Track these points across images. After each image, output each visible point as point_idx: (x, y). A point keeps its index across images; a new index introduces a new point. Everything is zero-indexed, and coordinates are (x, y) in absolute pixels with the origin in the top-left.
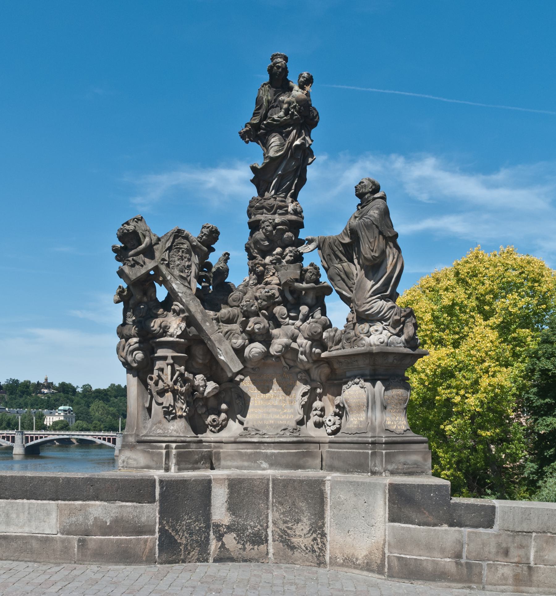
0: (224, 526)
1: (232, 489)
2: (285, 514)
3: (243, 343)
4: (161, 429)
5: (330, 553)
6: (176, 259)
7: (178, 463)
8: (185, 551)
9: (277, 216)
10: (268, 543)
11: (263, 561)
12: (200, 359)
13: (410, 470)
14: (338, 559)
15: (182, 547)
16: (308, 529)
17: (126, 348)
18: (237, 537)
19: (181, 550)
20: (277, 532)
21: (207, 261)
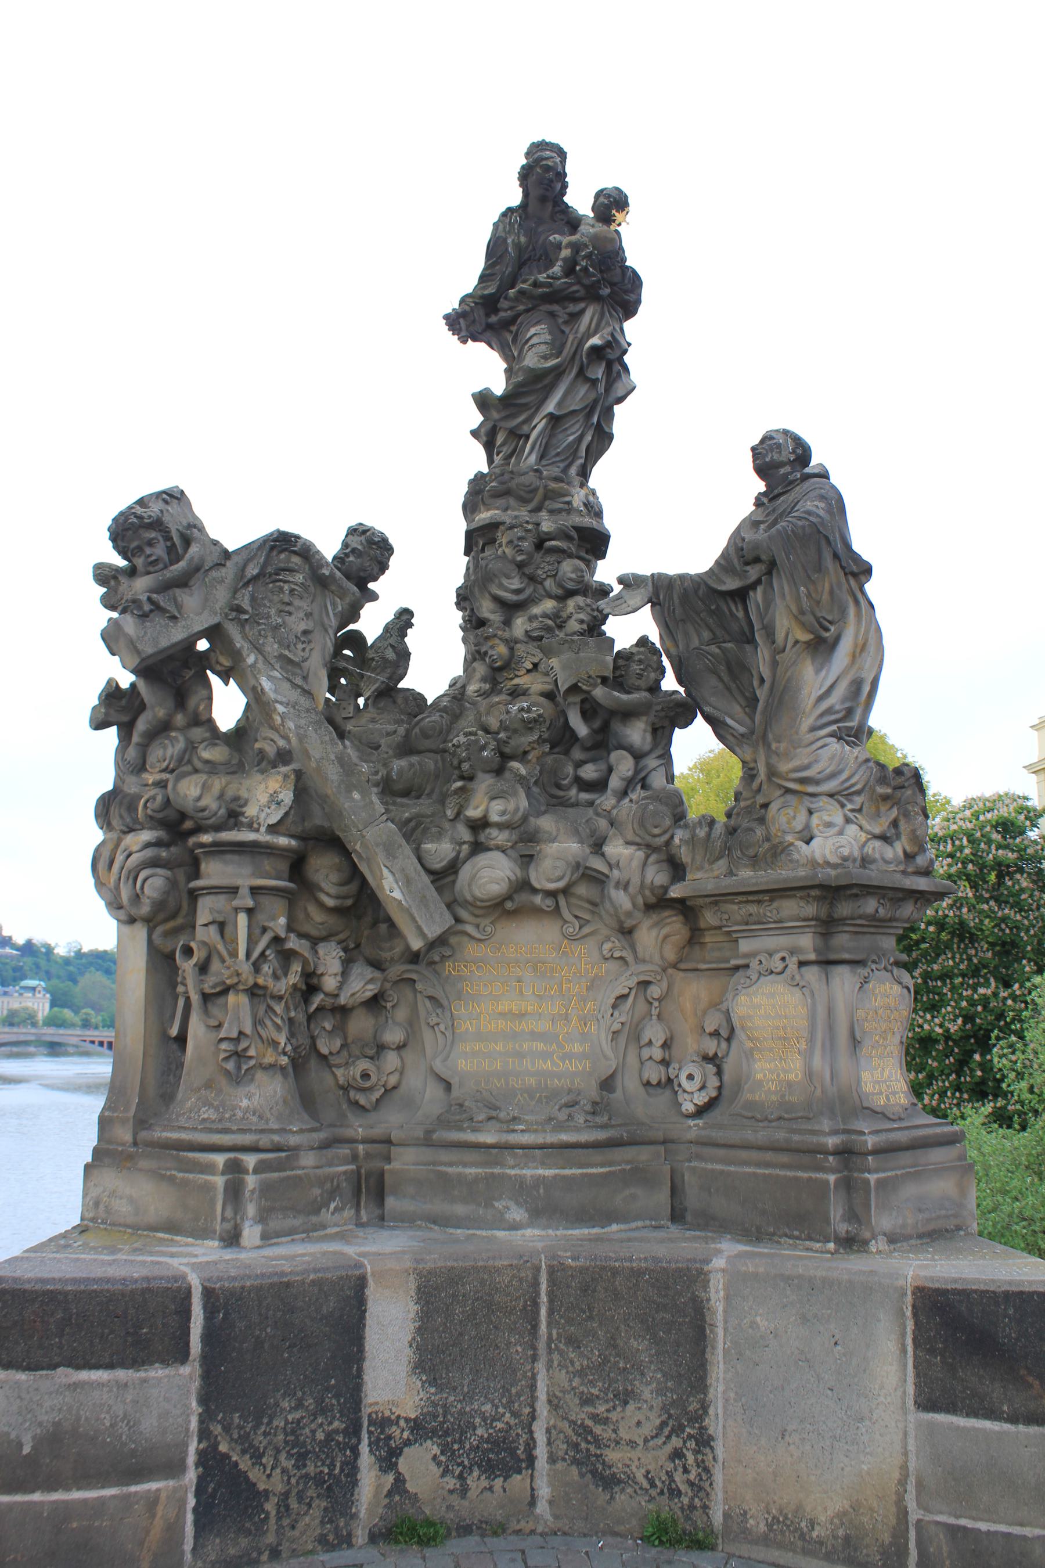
0: (402, 1423)
1: (427, 1302)
2: (587, 1375)
3: (454, 854)
4: (211, 1105)
5: (726, 1501)
6: (273, 612)
7: (262, 1218)
8: (279, 1518)
9: (544, 514)
10: (533, 1469)
11: (518, 1527)
12: (328, 894)
13: (931, 1227)
14: (751, 1521)
15: (270, 1507)
16: (658, 1422)
17: (120, 858)
18: (442, 1453)
19: (268, 1514)
20: (561, 1432)
21: (352, 627)
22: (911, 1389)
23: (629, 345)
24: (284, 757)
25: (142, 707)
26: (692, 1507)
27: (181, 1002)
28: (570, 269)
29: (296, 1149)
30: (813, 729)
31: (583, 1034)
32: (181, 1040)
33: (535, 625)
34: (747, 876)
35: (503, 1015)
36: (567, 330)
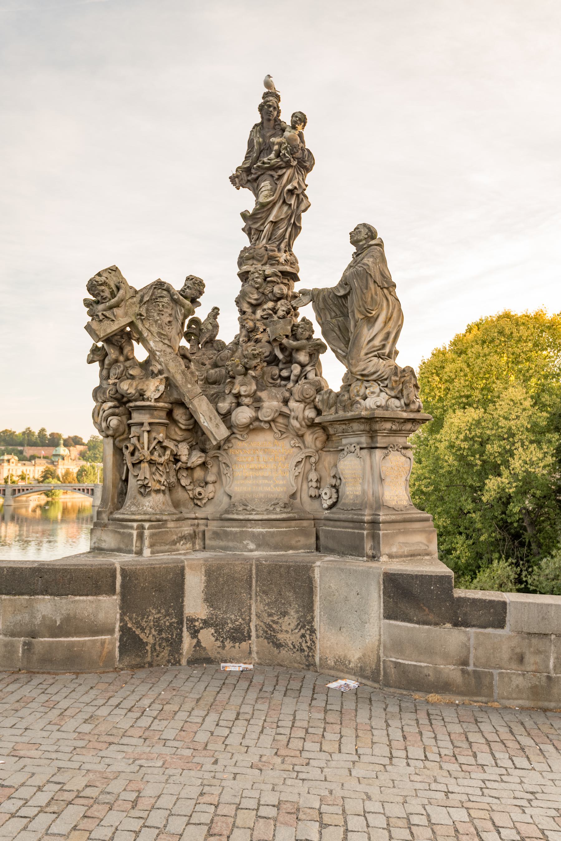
0: (200, 621)
4: (135, 505)
5: (320, 654)
7: (152, 546)
8: (152, 653)
15: (148, 648)
17: (101, 412)
19: (147, 650)
22: (382, 611)
23: (307, 186)
24: (160, 372)
25: (106, 355)
26: (308, 656)
27: (125, 468)
28: (278, 155)
29: (166, 521)
30: (367, 354)
31: (284, 477)
32: (126, 480)
33: (265, 313)
34: (341, 414)
35: (252, 469)
36: (278, 183)
